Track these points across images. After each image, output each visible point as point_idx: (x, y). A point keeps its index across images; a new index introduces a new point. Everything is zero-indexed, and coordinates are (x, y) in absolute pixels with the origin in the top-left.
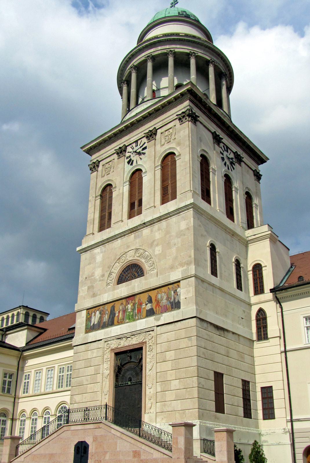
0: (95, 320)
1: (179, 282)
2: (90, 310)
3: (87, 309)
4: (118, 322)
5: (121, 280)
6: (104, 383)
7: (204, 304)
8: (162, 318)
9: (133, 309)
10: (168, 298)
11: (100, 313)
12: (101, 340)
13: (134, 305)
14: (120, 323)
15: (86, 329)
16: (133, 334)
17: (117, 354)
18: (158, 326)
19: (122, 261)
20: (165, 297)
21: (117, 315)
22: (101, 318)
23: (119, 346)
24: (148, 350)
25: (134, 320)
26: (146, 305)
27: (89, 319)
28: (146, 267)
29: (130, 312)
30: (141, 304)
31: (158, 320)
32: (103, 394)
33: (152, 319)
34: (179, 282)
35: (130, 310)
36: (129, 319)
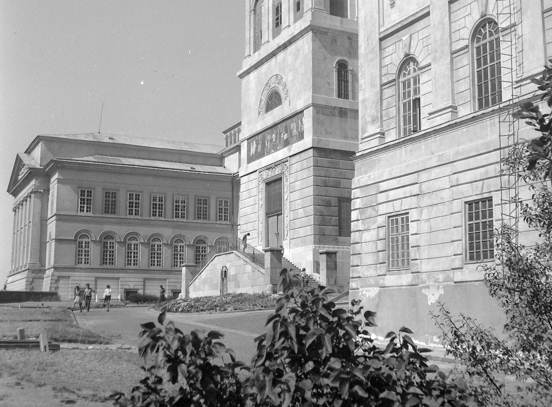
0: (253, 150)
1: (302, 111)
2: (250, 140)
3: (248, 139)
4: (267, 152)
5: (269, 108)
6: (260, 212)
7: (326, 131)
8: (293, 148)
9: (276, 139)
10: (297, 128)
11: (256, 143)
12: (256, 171)
13: (276, 135)
14: (269, 153)
15: (248, 159)
16: (276, 164)
17: (268, 184)
18: (290, 157)
19: (268, 88)
20: (295, 127)
21: (266, 145)
22: (257, 148)
23: (268, 177)
24: (285, 180)
25: (277, 151)
26: (284, 135)
27: (249, 150)
28: (283, 95)
29: (274, 142)
30: (280, 134)
31: (290, 150)
32: (260, 223)
33: (286, 149)
34: (302, 111)
35: (274, 140)
36: (274, 149)
